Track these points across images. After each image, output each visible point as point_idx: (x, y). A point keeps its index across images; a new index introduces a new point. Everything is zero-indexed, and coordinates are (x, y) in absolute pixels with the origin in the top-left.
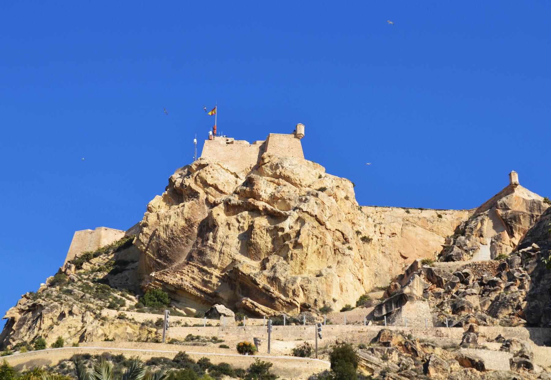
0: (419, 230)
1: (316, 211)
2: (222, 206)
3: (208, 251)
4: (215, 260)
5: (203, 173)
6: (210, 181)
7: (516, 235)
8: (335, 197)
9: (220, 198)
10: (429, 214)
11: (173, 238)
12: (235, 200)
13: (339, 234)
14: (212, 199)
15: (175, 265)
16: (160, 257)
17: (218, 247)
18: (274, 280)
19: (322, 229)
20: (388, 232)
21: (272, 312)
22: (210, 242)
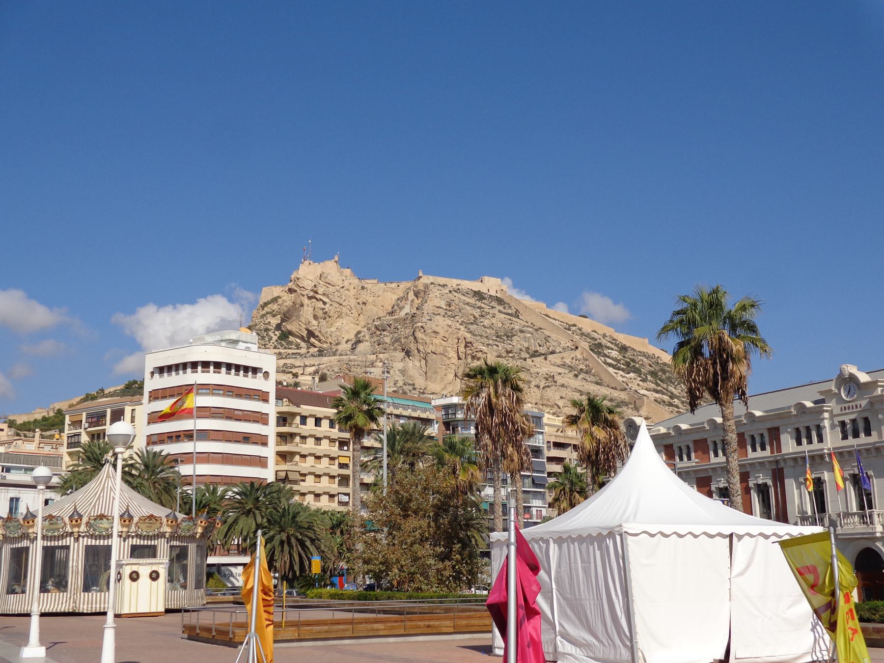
0: (389, 293)
1: (337, 300)
2: (306, 296)
3: (301, 317)
4: (303, 321)
5: (298, 283)
6: (301, 286)
7: (419, 299)
8: (348, 290)
9: (305, 293)
10: (394, 285)
11: (289, 310)
12: (311, 294)
13: (349, 307)
14: (303, 293)
15: (291, 320)
16: (286, 317)
17: (304, 315)
18: (320, 332)
19: (341, 307)
20: (376, 296)
21: (320, 345)
22: (302, 312)
